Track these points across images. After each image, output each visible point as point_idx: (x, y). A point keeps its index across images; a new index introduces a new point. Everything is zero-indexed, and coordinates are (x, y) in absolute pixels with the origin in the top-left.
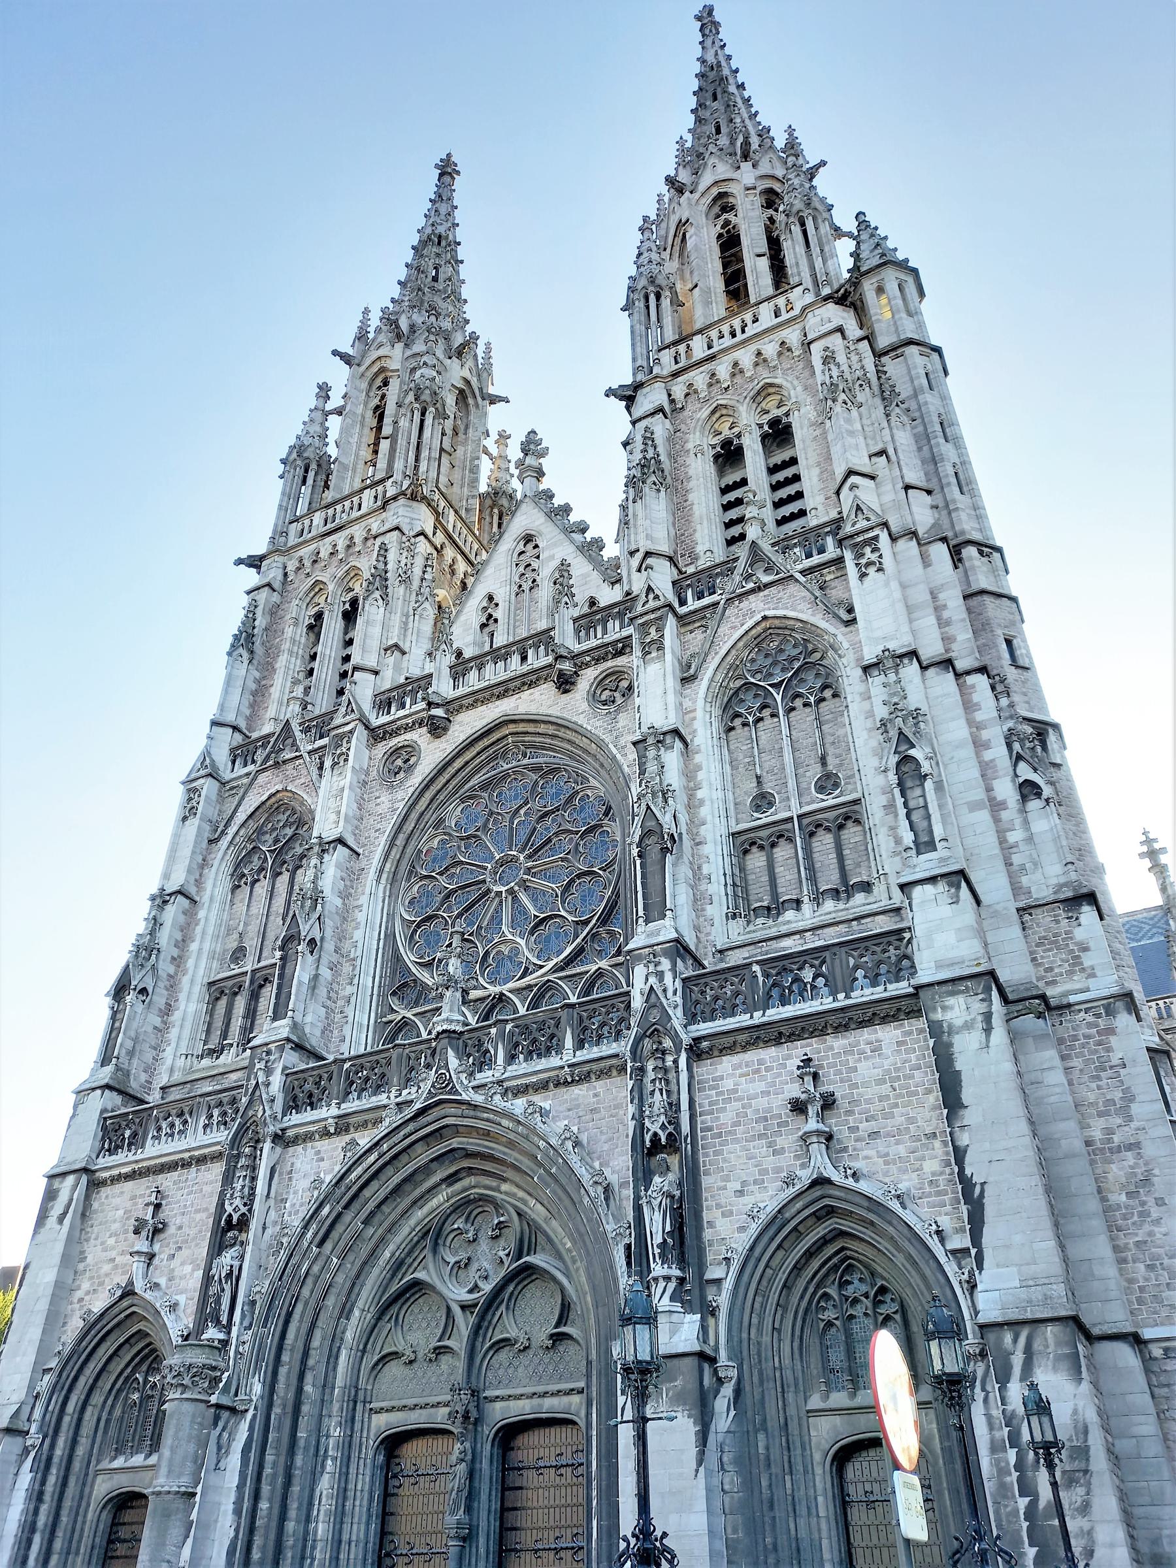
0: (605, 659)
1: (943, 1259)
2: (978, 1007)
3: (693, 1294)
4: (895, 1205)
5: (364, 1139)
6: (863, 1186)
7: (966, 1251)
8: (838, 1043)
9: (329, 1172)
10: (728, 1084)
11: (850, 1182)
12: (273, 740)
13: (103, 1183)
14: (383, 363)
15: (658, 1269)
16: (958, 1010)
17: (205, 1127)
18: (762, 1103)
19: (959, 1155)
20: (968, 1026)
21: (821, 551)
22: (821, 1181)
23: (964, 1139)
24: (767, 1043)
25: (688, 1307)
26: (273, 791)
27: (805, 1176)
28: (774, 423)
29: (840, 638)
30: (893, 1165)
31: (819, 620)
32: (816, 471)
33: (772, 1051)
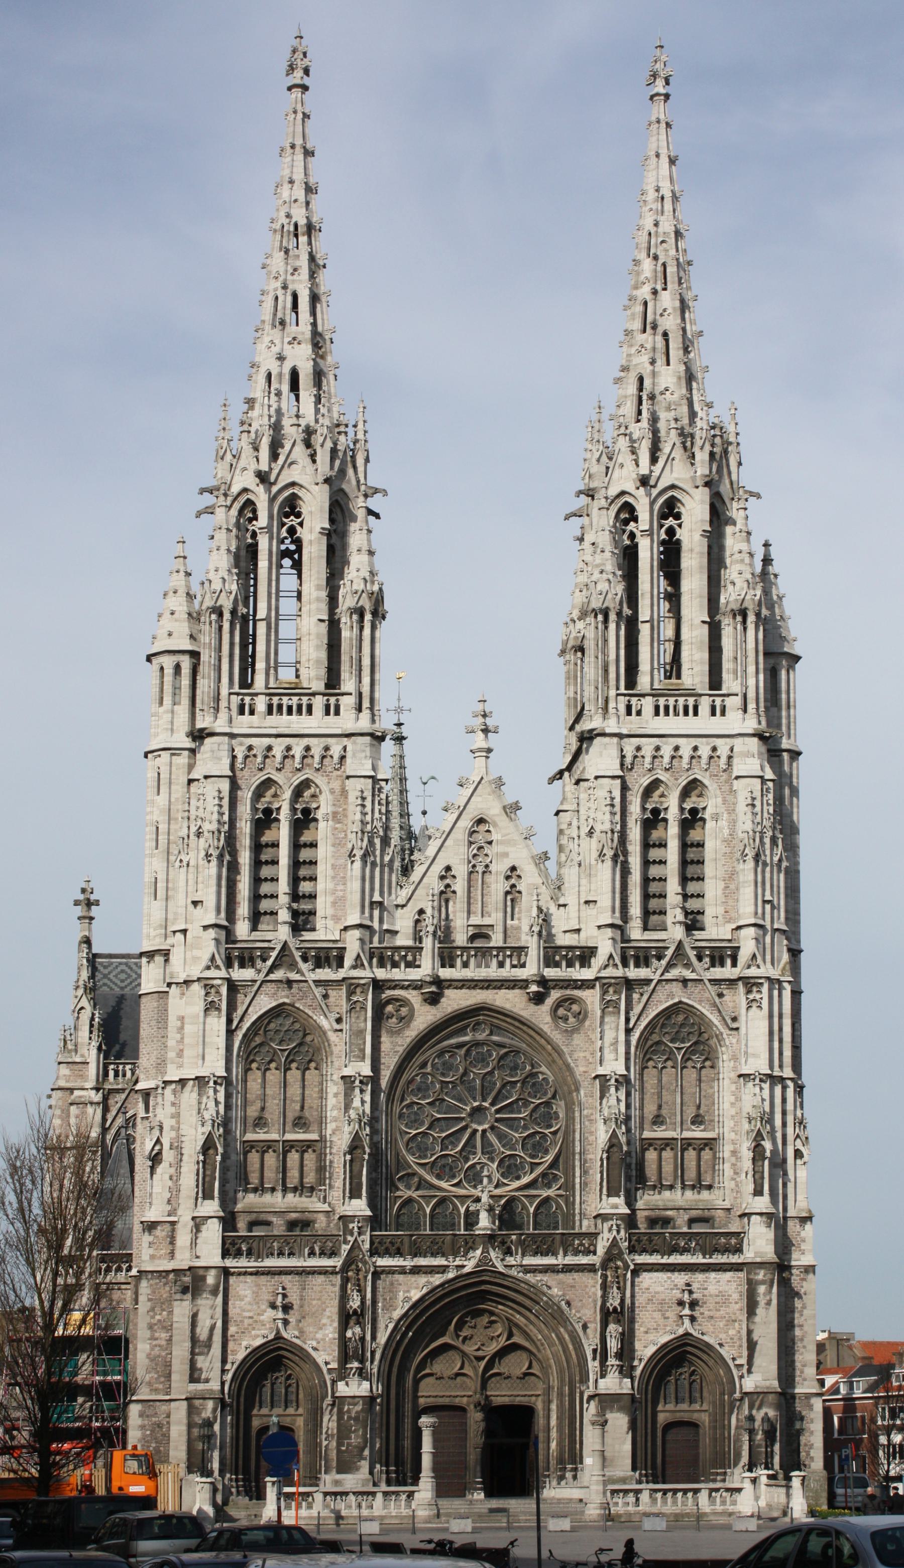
0: (566, 988)
1: (732, 1367)
2: (769, 1276)
3: (626, 1371)
4: (718, 1347)
5: (437, 1279)
6: (705, 1338)
7: (742, 1365)
8: (700, 1276)
9: (416, 1295)
10: (644, 1285)
11: (700, 1336)
12: (274, 954)
13: (233, 1274)
14: (296, 490)
15: (612, 1361)
16: (761, 1275)
17: (309, 1255)
18: (662, 1296)
19: (749, 1332)
20: (763, 1282)
21: (722, 965)
22: (687, 1334)
23: (752, 1327)
24: (668, 1271)
25: (625, 1377)
26: (281, 1001)
27: (681, 1331)
28: (694, 811)
29: (725, 1036)
30: (721, 1331)
31: (714, 1019)
32: (721, 885)
33: (669, 1274)
